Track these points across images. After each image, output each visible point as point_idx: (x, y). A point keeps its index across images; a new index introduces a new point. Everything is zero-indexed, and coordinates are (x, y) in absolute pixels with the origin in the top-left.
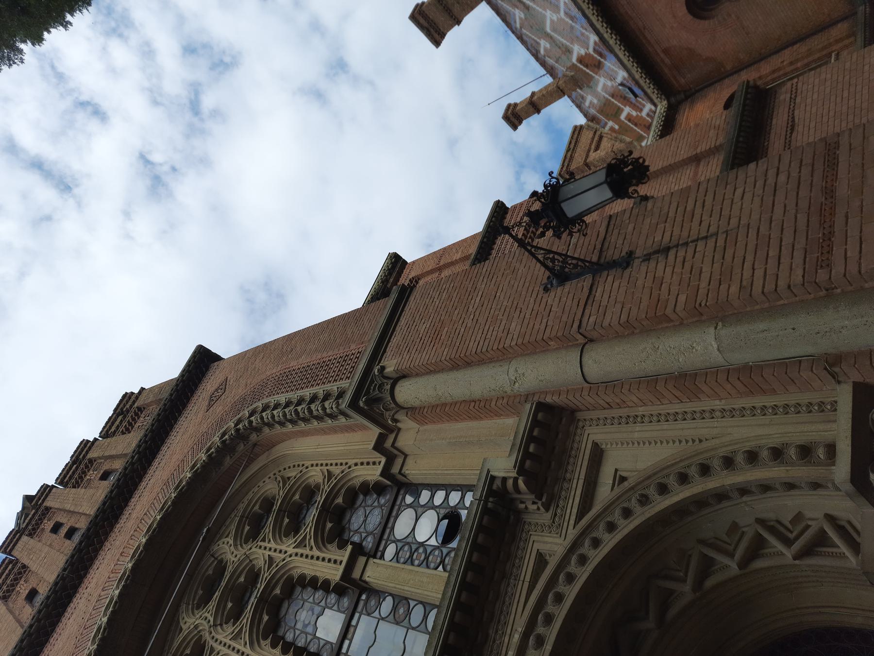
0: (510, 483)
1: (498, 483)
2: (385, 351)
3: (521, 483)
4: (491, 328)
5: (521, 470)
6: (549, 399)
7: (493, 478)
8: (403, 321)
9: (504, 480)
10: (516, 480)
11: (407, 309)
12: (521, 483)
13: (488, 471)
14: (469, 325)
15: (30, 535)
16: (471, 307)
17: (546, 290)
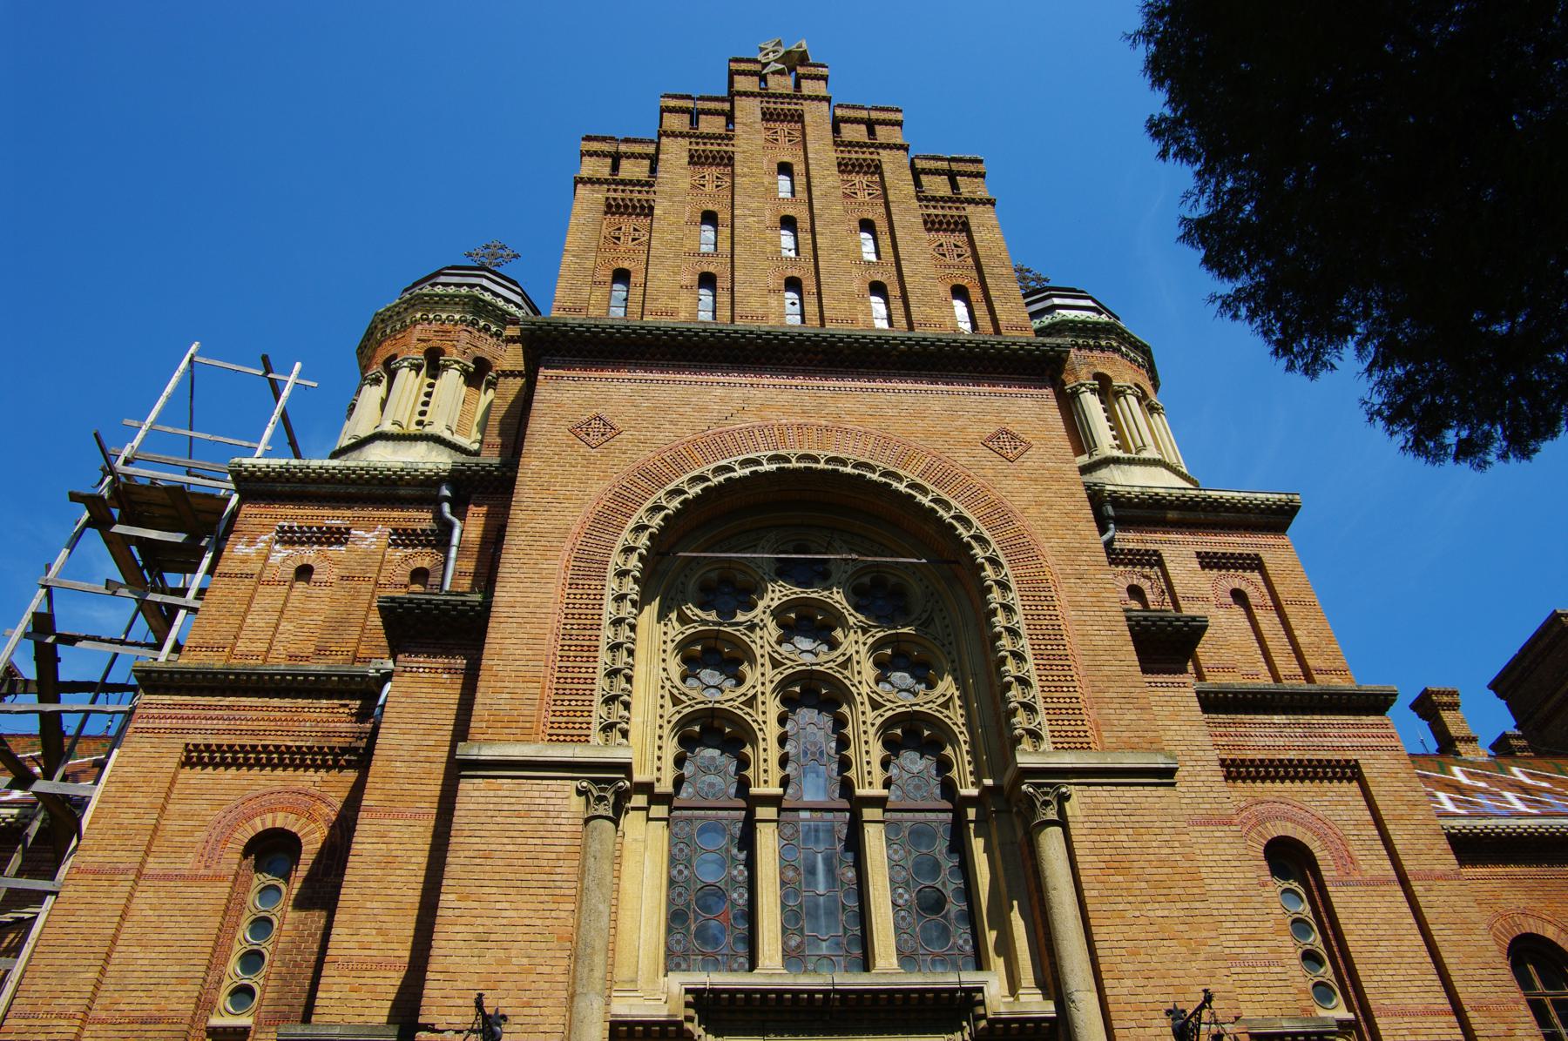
0: (981, 1011)
1: (979, 996)
2: (1089, 785)
3: (983, 1023)
4: (1123, 952)
5: (992, 1022)
6: (1061, 1029)
7: (981, 990)
8: (1129, 793)
9: (982, 1003)
10: (984, 1016)
11: (1148, 790)
12: (983, 1023)
13: (985, 982)
14: (1129, 914)
15: (768, 116)
16: (1149, 906)
17: (1169, 1012)
